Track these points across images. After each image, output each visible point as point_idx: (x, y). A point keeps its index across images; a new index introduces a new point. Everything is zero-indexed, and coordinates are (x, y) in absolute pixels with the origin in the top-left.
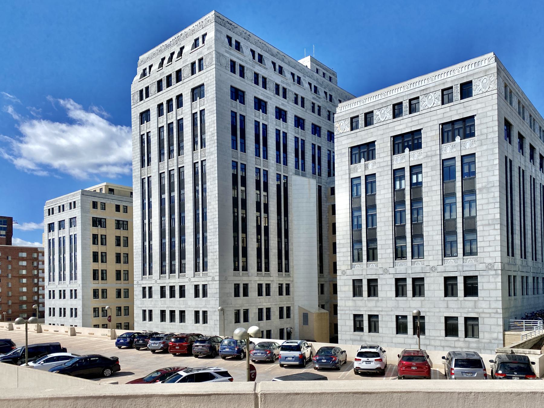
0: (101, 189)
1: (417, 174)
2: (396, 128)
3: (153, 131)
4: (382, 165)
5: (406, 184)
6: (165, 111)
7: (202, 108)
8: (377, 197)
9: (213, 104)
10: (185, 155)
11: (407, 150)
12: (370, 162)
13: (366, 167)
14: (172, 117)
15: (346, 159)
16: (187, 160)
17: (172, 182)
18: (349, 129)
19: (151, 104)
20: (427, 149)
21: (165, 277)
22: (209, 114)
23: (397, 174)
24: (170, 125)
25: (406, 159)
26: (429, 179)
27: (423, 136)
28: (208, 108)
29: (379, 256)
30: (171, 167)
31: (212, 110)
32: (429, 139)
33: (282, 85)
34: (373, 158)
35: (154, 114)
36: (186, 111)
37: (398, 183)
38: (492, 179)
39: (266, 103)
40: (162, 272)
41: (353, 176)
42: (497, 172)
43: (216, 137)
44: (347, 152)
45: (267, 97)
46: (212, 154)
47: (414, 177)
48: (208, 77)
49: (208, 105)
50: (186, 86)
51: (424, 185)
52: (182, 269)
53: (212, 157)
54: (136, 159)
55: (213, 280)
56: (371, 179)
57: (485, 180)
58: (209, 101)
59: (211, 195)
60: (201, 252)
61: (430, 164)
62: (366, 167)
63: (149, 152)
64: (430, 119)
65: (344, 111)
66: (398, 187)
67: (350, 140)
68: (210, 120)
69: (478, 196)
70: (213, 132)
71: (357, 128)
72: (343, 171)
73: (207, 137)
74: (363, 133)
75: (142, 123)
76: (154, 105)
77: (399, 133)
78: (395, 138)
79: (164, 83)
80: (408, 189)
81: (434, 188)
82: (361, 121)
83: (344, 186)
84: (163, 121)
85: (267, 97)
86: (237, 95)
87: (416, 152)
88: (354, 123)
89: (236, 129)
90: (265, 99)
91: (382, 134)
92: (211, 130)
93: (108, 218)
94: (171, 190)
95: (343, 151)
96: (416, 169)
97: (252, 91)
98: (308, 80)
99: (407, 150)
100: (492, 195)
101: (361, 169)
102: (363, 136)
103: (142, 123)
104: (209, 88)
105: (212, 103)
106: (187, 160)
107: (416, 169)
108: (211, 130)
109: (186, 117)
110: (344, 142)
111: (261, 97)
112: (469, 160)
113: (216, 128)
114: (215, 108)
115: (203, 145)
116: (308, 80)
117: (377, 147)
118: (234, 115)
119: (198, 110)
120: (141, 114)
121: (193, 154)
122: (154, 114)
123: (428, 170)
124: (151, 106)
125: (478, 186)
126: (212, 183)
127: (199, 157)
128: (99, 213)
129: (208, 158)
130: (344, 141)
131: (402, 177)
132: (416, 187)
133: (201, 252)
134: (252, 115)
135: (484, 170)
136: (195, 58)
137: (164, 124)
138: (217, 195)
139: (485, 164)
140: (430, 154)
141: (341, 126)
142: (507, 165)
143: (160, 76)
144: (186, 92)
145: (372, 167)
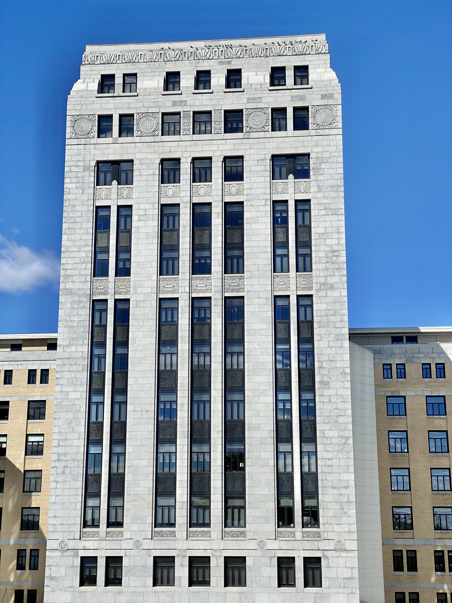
3: (142, 206)
9: (334, 198)
10: (246, 274)
19: (144, 152)
22: (323, 212)
28: (321, 201)
30: (200, 291)
31: (332, 207)
36: (253, 191)
43: (344, 259)
46: (332, 287)
49: (320, 195)
50: (257, 146)
53: (330, 293)
54: (76, 254)
58: (325, 190)
59: (330, 369)
68: (328, 224)
70: (335, 248)
76: (149, 156)
84: (183, 193)
92: (329, 242)
94: (200, 341)
104: (323, 166)
105: (334, 194)
108: (329, 242)
109: (254, 203)
113: (343, 242)
114: (342, 206)
121: (273, 278)
124: (139, 156)
126: (332, 344)
127: (293, 287)
129: (322, 293)
136: (287, 99)
138: (348, 371)
143: (174, 104)
144: (253, 157)
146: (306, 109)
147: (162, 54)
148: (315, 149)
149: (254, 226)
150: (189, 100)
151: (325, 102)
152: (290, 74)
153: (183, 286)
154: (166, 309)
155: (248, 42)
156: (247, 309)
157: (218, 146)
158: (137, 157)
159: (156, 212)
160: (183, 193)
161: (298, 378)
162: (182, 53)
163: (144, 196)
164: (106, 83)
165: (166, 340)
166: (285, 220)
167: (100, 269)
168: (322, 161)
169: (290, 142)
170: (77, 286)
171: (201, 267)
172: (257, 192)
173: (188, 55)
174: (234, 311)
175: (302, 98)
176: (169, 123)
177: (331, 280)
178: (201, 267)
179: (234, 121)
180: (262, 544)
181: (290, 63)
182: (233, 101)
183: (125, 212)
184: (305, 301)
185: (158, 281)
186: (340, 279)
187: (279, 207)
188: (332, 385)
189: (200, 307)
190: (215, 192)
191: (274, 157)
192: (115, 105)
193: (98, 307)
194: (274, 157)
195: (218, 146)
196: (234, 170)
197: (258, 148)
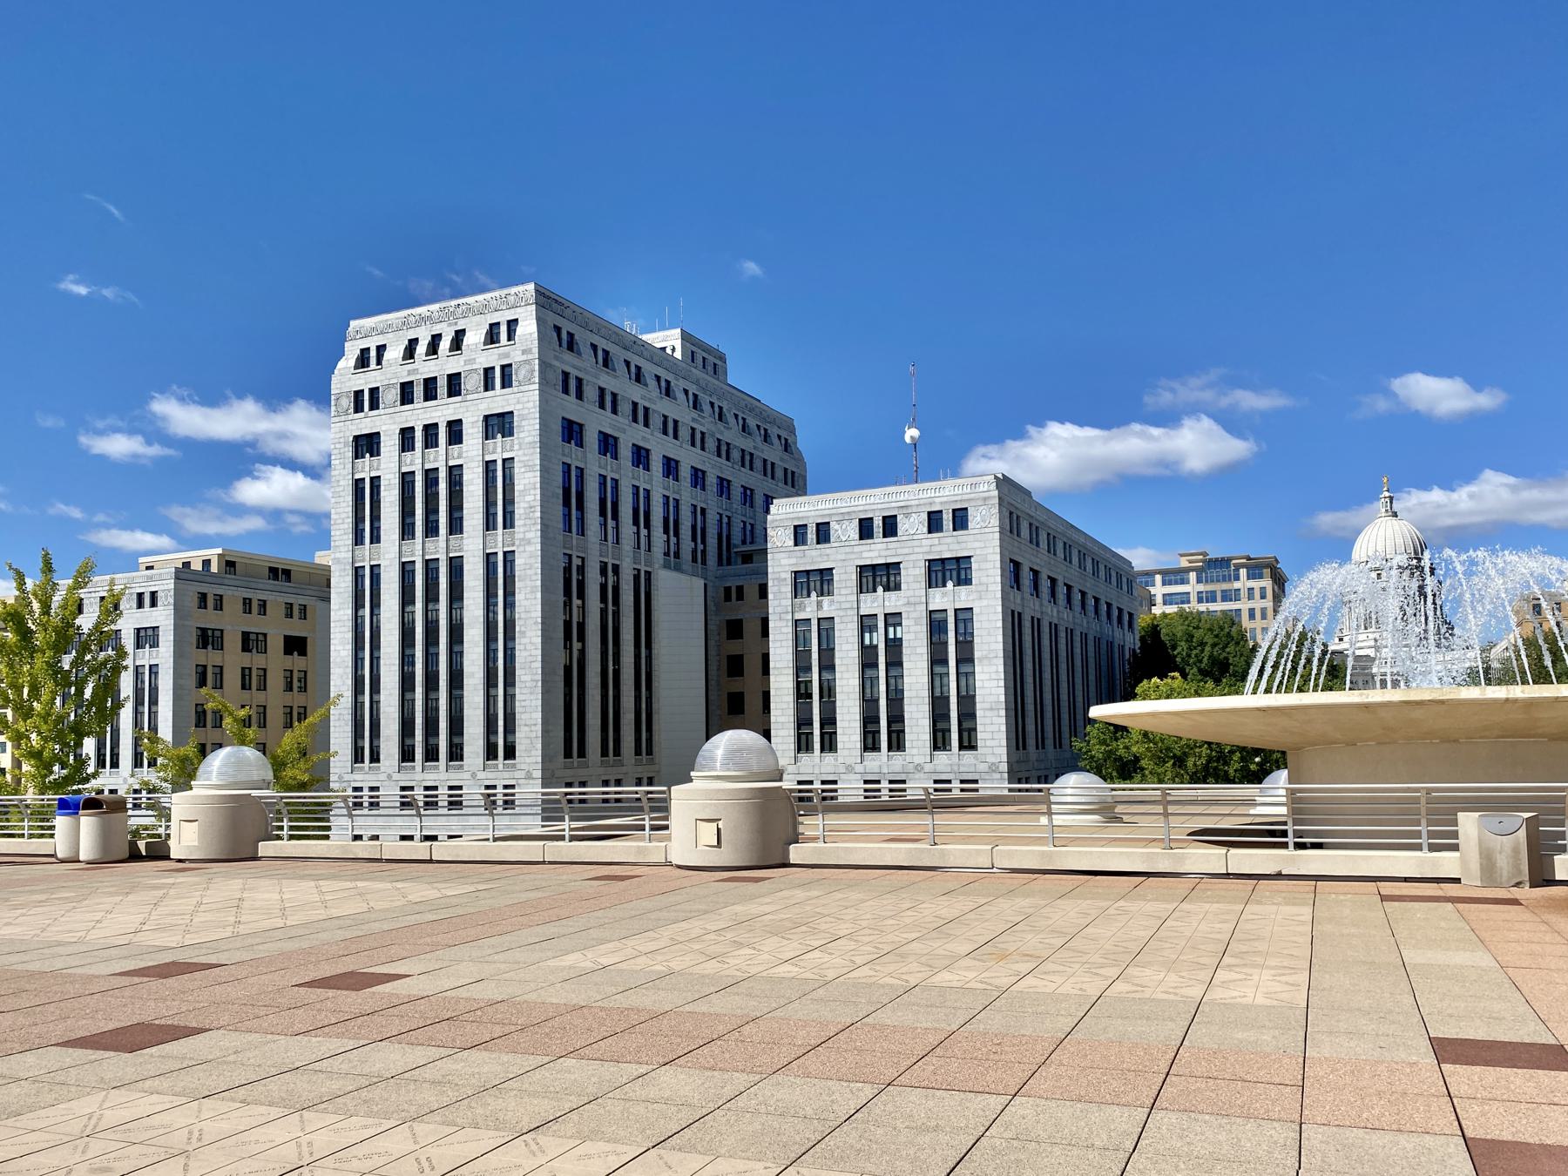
0: (206, 563)
1: (895, 626)
2: (865, 555)
4: (843, 606)
5: (879, 639)
6: (419, 443)
7: (506, 456)
8: (837, 654)
11: (880, 589)
12: (826, 600)
13: (819, 605)
14: (439, 458)
15: (788, 589)
16: (472, 545)
17: (434, 585)
18: (791, 543)
19: (387, 422)
20: (911, 593)
21: (437, 767)
23: (866, 624)
24: (431, 477)
25: (878, 603)
26: (912, 636)
27: (903, 572)
29: (839, 746)
32: (911, 579)
33: (642, 403)
34: (830, 593)
35: (390, 444)
37: (867, 635)
38: (993, 646)
39: (616, 439)
40: (407, 755)
41: (798, 616)
42: (1000, 638)
44: (788, 577)
45: (619, 429)
46: (529, 542)
47: (891, 630)
48: (524, 401)
51: (905, 644)
52: (456, 753)
53: (528, 548)
55: (529, 776)
56: (826, 628)
57: (986, 647)
60: (501, 723)
61: (914, 615)
62: (819, 605)
63: (376, 517)
64: (913, 549)
65: (784, 512)
66: (867, 642)
67: (793, 561)
69: (977, 669)
71: (804, 543)
72: (781, 606)
73: (520, 509)
74: (814, 553)
75: (358, 455)
77: (869, 562)
78: (862, 569)
79: (419, 391)
80: (882, 647)
81: (919, 650)
82: (811, 535)
83: (785, 630)
84: (415, 462)
85: (619, 429)
86: (572, 432)
87: (892, 595)
88: (799, 534)
89: (567, 495)
90: (616, 434)
91: (845, 556)
92: (529, 498)
93: (227, 628)
95: (783, 575)
96: (893, 619)
97: (596, 421)
98: (682, 384)
99: (880, 589)
100: (994, 668)
101: (810, 608)
102: (814, 557)
103: (358, 455)
106: (472, 545)
107: (893, 619)
108: (529, 498)
110: (784, 562)
111: (609, 431)
112: (964, 617)
115: (509, 523)
116: (682, 384)
117: (836, 578)
118: (567, 468)
119: (499, 458)
120: (357, 438)
122: (390, 444)
123: (911, 622)
125: (977, 654)
128: (210, 619)
130: (782, 560)
131: (873, 629)
132: (894, 646)
133: (501, 723)
134: (594, 464)
135: (984, 633)
137: (417, 468)
139: (985, 625)
140: (912, 600)
141: (779, 537)
142: (1014, 622)
145: (828, 607)
146: (510, 365)
147: (405, 324)
148: (519, 406)
149: (471, 488)
150: (425, 367)
151: (524, 357)
152: (504, 329)
153: (416, 551)
154: (406, 571)
155: (470, 300)
156: (466, 568)
157: (441, 411)
158: (382, 429)
159: (396, 481)
160: (415, 462)
161: (501, 632)
162: (423, 320)
163: (387, 466)
164: (363, 361)
165: (407, 597)
166: (495, 478)
167: (358, 539)
168: (523, 418)
169: (498, 401)
170: (343, 555)
171: (431, 530)
172: (472, 453)
173: (426, 320)
174: (456, 566)
175: (507, 355)
176: (406, 394)
177: (529, 535)
178: (431, 530)
179: (455, 384)
180: (474, 775)
181: (502, 317)
182: (452, 365)
183: (375, 481)
184: (509, 557)
185: (400, 546)
186: (535, 535)
187: (489, 466)
188: (528, 634)
189: (431, 567)
190: (439, 458)
191: (486, 418)
192: (365, 381)
193: (358, 572)
194: (486, 418)
195: (441, 411)
196: (455, 432)
197: (472, 409)
